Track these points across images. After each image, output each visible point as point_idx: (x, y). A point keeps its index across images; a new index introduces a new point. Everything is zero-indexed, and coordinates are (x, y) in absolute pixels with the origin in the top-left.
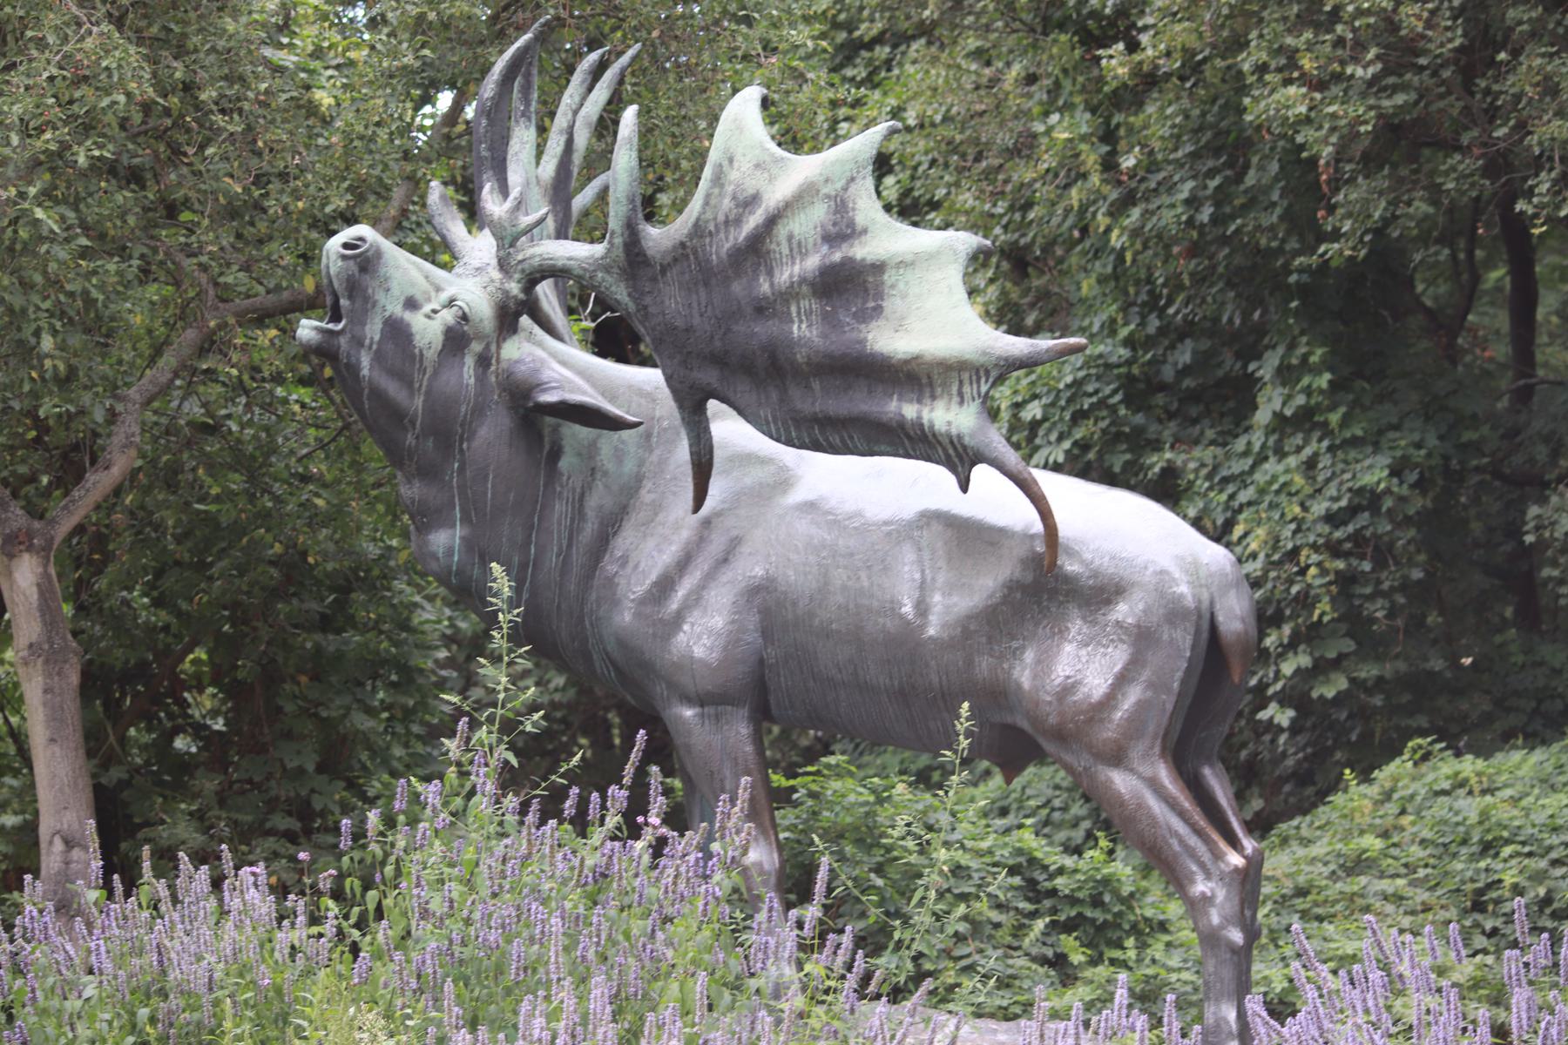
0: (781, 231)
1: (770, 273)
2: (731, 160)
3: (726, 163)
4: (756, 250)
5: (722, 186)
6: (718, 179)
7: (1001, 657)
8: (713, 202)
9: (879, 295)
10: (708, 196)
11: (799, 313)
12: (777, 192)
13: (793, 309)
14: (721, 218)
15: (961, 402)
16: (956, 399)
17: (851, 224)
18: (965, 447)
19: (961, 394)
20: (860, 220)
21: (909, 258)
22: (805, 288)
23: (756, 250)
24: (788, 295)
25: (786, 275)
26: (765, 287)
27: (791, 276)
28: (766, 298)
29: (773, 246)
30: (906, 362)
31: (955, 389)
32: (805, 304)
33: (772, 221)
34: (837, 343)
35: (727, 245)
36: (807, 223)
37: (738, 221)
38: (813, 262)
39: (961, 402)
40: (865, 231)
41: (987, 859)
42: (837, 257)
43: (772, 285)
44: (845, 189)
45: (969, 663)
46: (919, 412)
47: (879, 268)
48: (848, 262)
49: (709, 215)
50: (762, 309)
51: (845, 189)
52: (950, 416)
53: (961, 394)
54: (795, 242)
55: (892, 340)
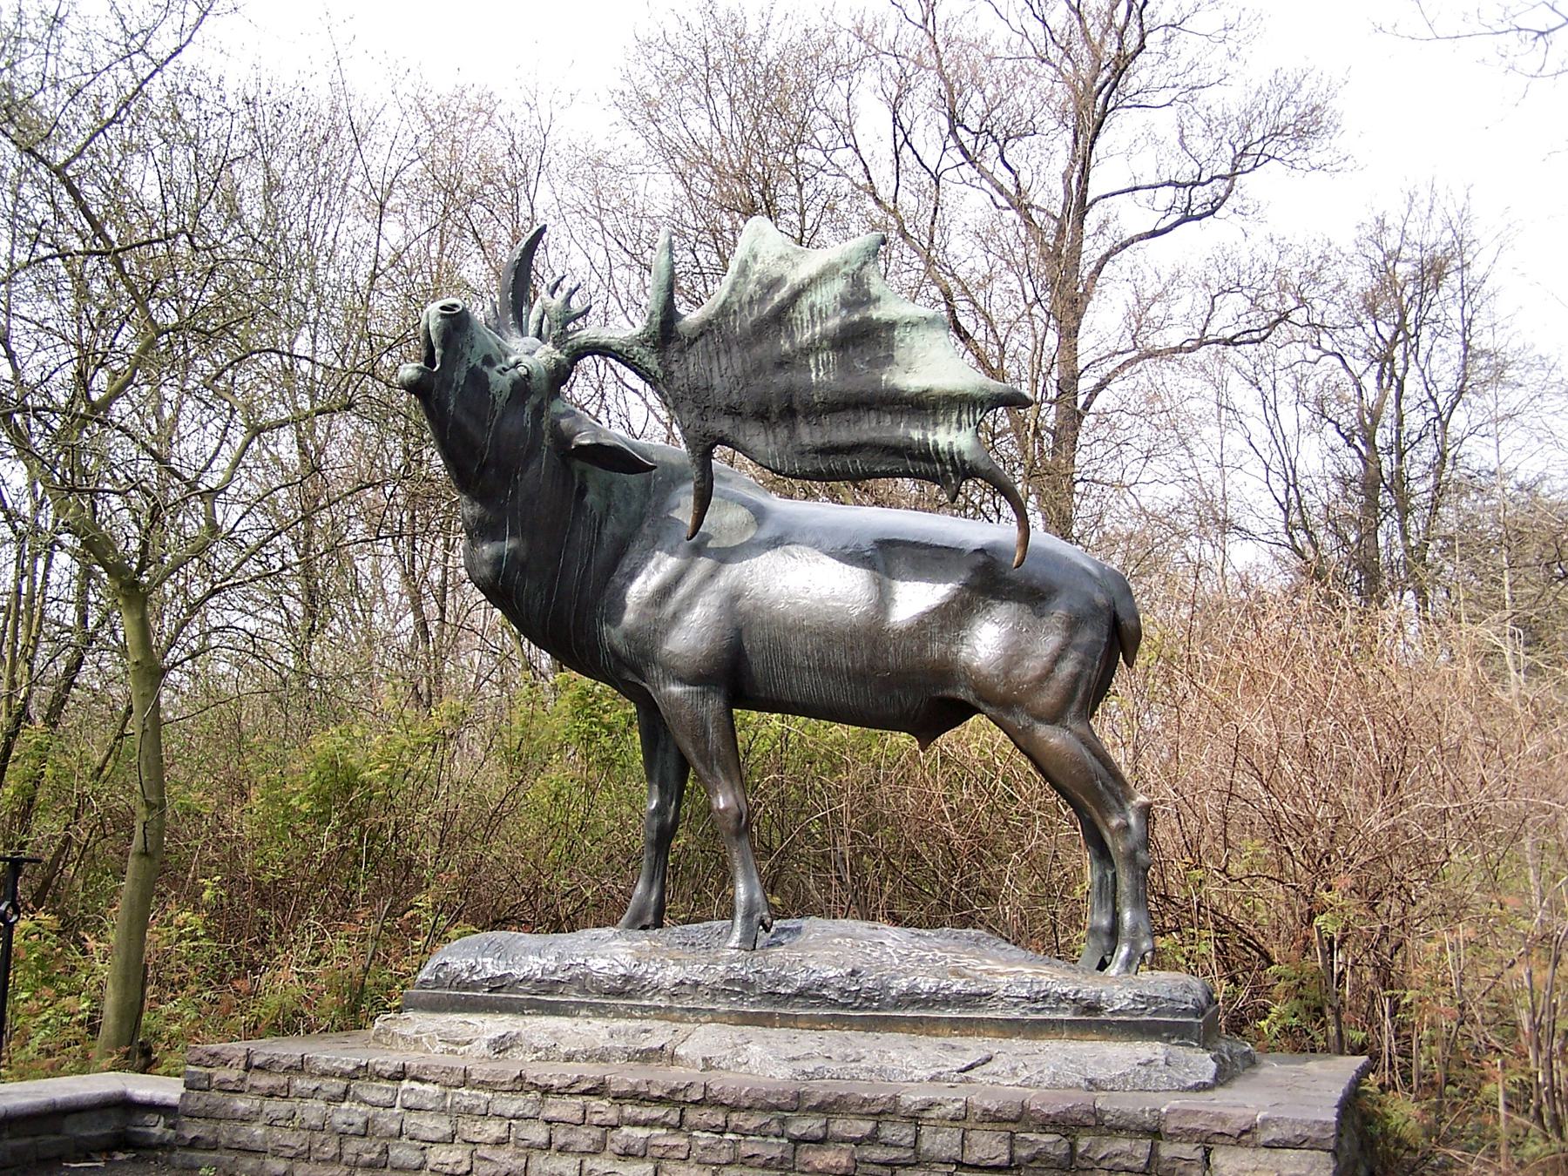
0: (804, 303)
1: (791, 336)
2: (755, 257)
3: (750, 260)
4: (780, 318)
5: (746, 276)
6: (743, 270)
7: (952, 642)
8: (738, 288)
9: (890, 346)
10: (735, 284)
11: (817, 365)
12: (796, 277)
13: (812, 362)
14: (746, 298)
15: (959, 429)
16: (955, 425)
17: (868, 293)
18: (963, 462)
19: (959, 422)
20: (874, 291)
21: (914, 320)
22: (825, 343)
23: (780, 318)
24: (810, 349)
25: (804, 336)
26: (786, 346)
27: (813, 335)
28: (786, 355)
29: (796, 314)
30: (918, 394)
31: (954, 418)
32: (822, 356)
33: (797, 295)
34: (857, 384)
35: (750, 319)
36: (827, 296)
37: (762, 300)
38: (833, 323)
39: (959, 429)
40: (878, 299)
41: (1377, 796)
42: (856, 317)
43: (792, 344)
44: (861, 269)
45: (922, 648)
46: (925, 435)
47: (891, 325)
48: (867, 321)
49: (734, 298)
50: (783, 363)
51: (861, 269)
52: (951, 438)
53: (959, 422)
54: (816, 311)
55: (909, 379)
